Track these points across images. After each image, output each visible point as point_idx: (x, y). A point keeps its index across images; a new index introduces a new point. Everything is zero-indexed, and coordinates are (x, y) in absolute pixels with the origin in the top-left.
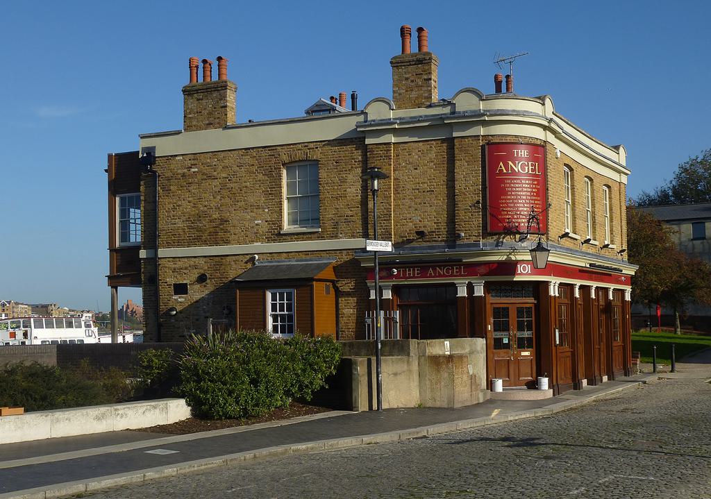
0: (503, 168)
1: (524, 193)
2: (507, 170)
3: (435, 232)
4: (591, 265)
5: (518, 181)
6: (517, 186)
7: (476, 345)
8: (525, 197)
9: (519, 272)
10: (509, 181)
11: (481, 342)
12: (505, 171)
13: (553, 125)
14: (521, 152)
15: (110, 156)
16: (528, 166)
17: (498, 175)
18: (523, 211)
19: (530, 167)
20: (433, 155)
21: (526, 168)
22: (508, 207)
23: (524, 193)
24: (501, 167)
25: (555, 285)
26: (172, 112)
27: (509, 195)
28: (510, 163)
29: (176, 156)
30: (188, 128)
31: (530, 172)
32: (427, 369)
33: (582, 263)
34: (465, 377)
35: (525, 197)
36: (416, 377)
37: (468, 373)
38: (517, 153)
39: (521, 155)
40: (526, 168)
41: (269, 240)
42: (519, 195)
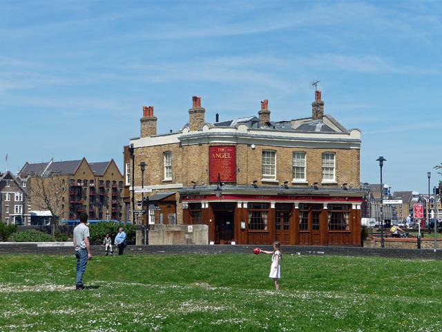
11: (206, 227)
15: (125, 147)
25: (242, 204)
26: (137, 128)
30: (142, 136)
32: (165, 235)
36: (162, 238)
41: (160, 184)
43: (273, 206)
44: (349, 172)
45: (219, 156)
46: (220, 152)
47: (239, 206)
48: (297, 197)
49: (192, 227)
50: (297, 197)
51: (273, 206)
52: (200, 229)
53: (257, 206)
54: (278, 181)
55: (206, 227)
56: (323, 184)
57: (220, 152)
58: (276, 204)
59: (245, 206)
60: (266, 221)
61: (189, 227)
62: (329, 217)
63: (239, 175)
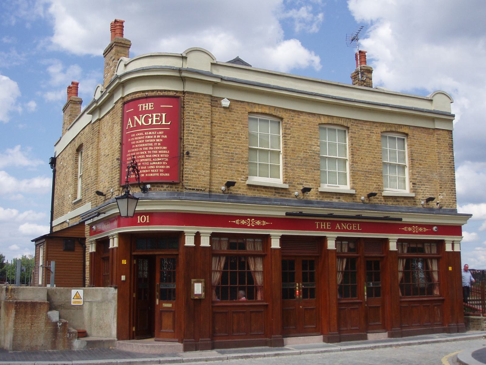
1: (146, 145)
2: (133, 125)
3: (107, 191)
4: (287, 214)
7: (108, 294)
8: (147, 149)
9: (139, 222)
10: (134, 135)
11: (112, 292)
13: (184, 74)
14: (146, 105)
16: (152, 116)
17: (127, 130)
18: (144, 162)
19: (155, 119)
20: (110, 124)
21: (150, 120)
23: (146, 145)
24: (129, 123)
27: (134, 148)
28: (136, 118)
29: (59, 155)
31: (154, 123)
33: (281, 213)
34: (41, 324)
35: (147, 149)
37: (48, 319)
38: (142, 107)
39: (145, 108)
40: (150, 120)
41: (73, 209)
42: (141, 147)
43: (275, 244)
44: (436, 177)
46: (143, 112)
47: (189, 242)
48: (334, 222)
49: (81, 292)
50: (334, 222)
51: (275, 244)
52: (99, 298)
53: (236, 242)
54: (286, 186)
55: (112, 292)
56: (386, 197)
57: (143, 112)
58: (283, 239)
59: (205, 242)
60: (259, 279)
61: (74, 292)
62: (401, 268)
63: (189, 165)
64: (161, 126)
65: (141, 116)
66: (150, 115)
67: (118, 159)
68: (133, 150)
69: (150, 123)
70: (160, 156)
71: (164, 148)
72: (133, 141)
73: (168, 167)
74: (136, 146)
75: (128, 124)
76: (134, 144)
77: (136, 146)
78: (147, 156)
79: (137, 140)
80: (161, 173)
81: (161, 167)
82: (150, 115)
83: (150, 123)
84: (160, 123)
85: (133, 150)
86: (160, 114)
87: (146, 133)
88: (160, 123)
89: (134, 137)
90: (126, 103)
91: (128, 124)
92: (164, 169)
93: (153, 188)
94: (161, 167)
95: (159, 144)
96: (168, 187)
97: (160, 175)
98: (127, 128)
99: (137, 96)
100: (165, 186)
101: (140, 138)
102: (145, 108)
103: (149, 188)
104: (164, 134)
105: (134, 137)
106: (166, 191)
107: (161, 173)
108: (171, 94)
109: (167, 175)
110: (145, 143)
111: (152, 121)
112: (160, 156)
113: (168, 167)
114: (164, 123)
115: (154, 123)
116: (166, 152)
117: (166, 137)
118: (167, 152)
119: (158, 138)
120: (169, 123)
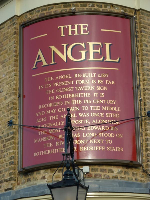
0: (43, 59)
1: (78, 95)
2: (48, 59)
5: (67, 76)
6: (64, 83)
8: (79, 102)
10: (51, 79)
12: (45, 63)
14: (73, 27)
16: (87, 47)
22: (49, 121)
23: (78, 95)
24: (39, 57)
28: (53, 48)
35: (79, 102)
38: (66, 30)
40: (83, 53)
45: (66, 55)
64: (104, 63)
65: (65, 45)
66: (83, 45)
67: (10, 123)
68: (51, 105)
69: (83, 57)
70: (105, 115)
71: (111, 102)
72: (50, 89)
73: (120, 136)
74: (58, 97)
75: (36, 61)
76: (51, 95)
77: (58, 97)
78: (81, 115)
79: (59, 87)
80: (109, 145)
81: (108, 135)
82: (83, 45)
83: (83, 57)
84: (101, 59)
85: (51, 105)
86: (100, 43)
87: (76, 76)
88: (101, 59)
89: (52, 82)
90: (27, 26)
91: (36, 61)
92: (114, 139)
93: (93, 173)
94: (108, 135)
95: (102, 95)
96: (121, 172)
97: (106, 149)
98: (34, 67)
99: (53, 11)
100: (116, 170)
101: (64, 83)
102: (73, 32)
103: (87, 173)
104: (109, 78)
105: (52, 82)
106: (116, 180)
107: (109, 145)
108: (116, 10)
109: (118, 149)
110: (75, 92)
111: (87, 54)
112: (105, 115)
113: (120, 136)
114: (108, 59)
115: (91, 58)
116: (115, 109)
117: (113, 82)
118: (117, 109)
119: (100, 85)
120: (117, 60)
